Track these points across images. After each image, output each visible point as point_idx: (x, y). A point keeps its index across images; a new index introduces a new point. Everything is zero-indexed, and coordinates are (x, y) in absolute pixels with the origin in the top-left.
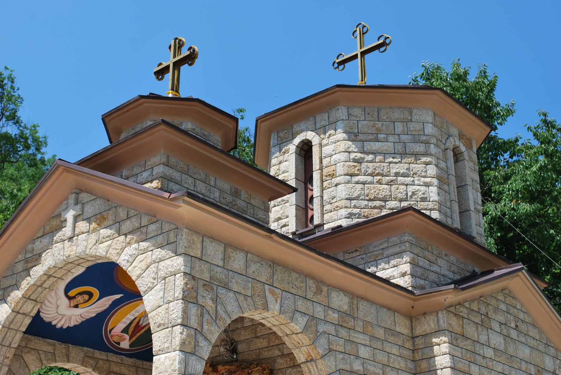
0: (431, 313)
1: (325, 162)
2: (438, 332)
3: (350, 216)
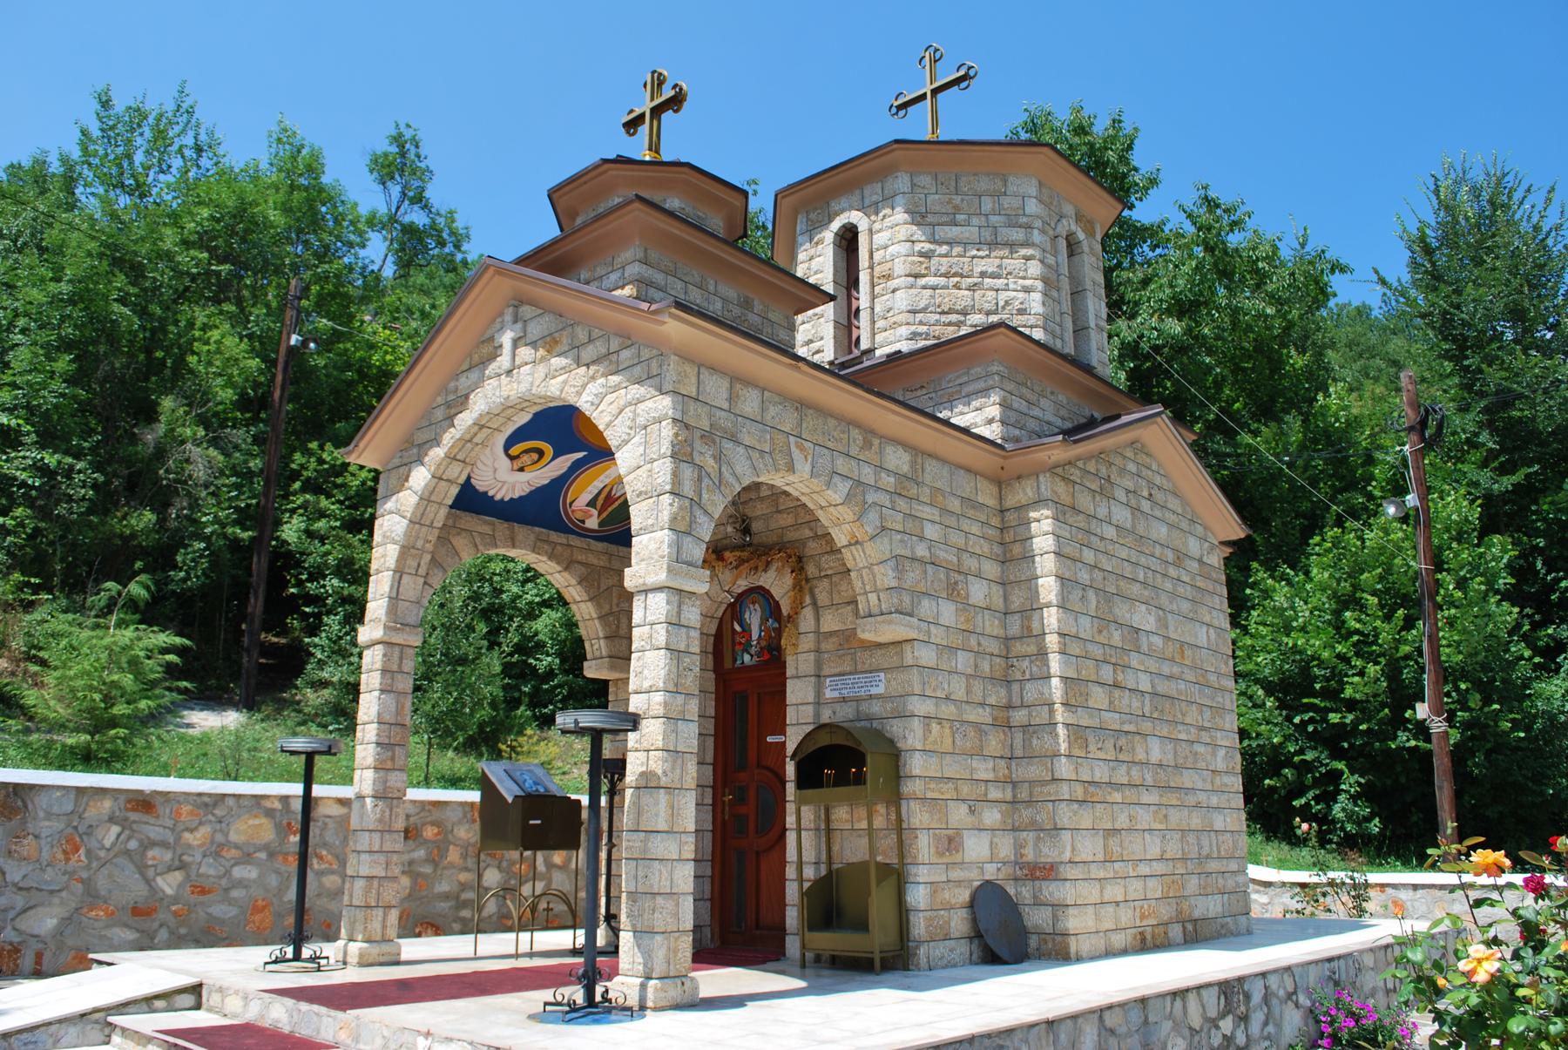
0: (1028, 476)
1: (877, 256)
2: (1038, 503)
3: (914, 336)
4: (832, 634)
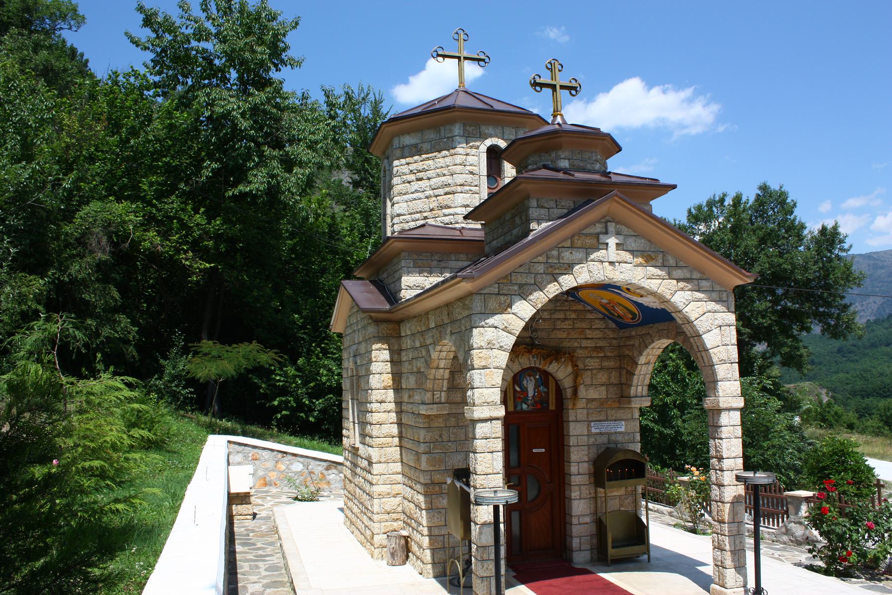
4: (593, 400)
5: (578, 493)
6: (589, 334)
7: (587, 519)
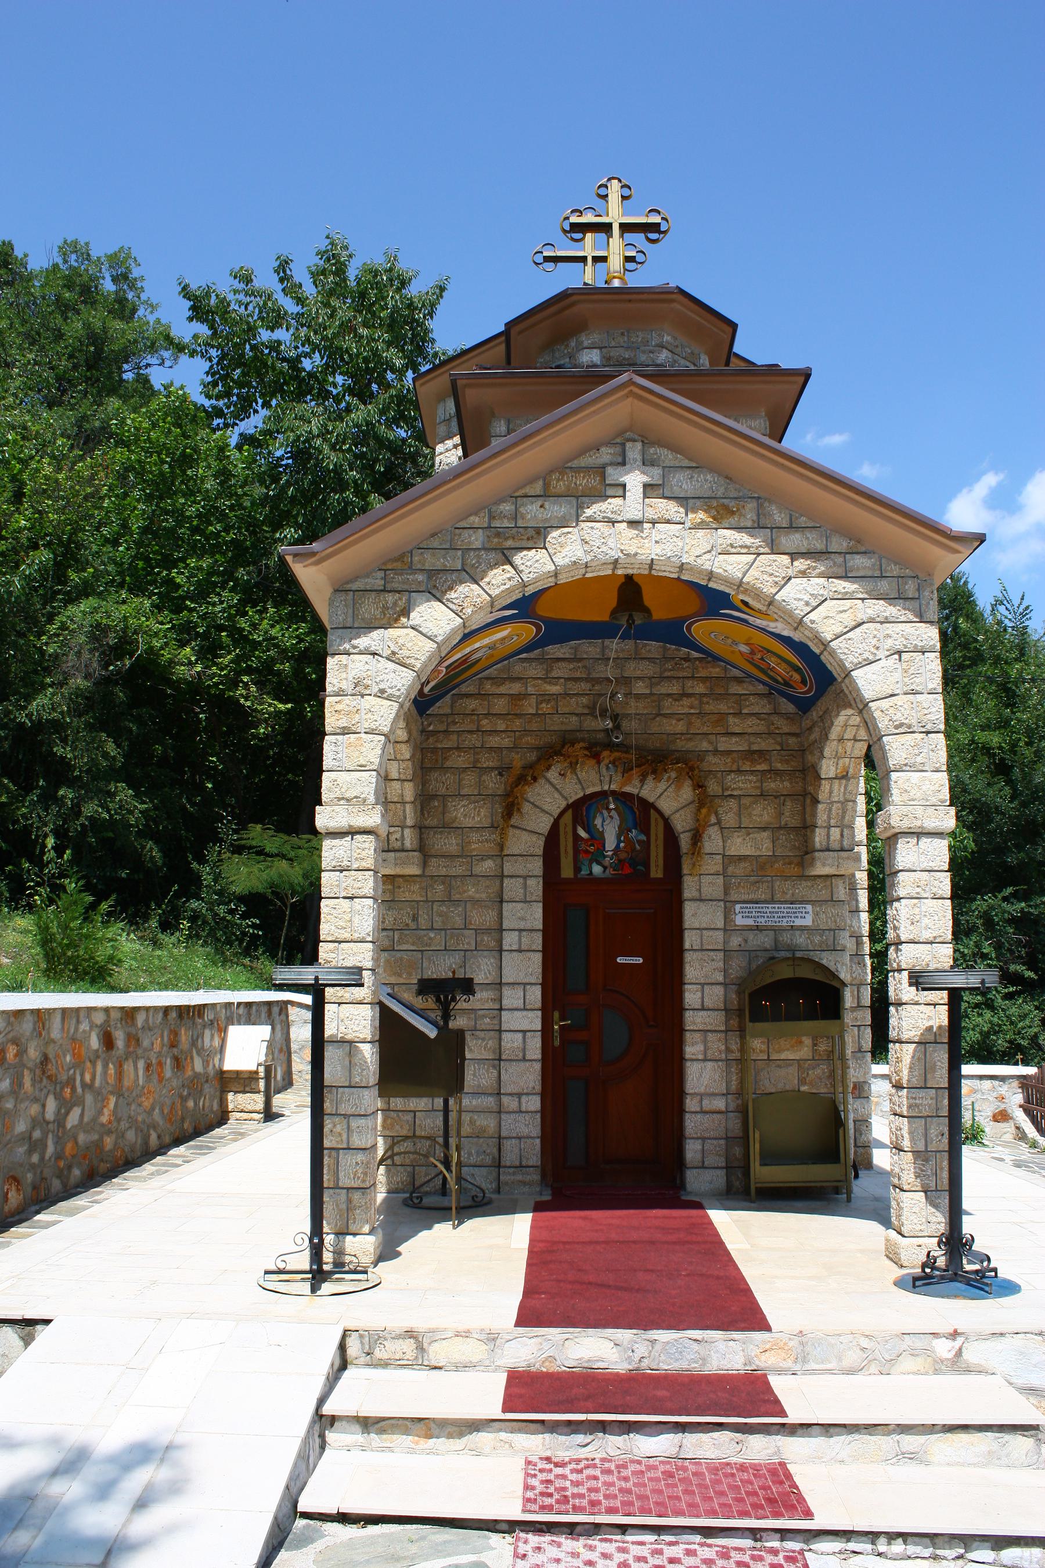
4: (742, 858)
5: (700, 1047)
6: (735, 724)
7: (720, 1104)
